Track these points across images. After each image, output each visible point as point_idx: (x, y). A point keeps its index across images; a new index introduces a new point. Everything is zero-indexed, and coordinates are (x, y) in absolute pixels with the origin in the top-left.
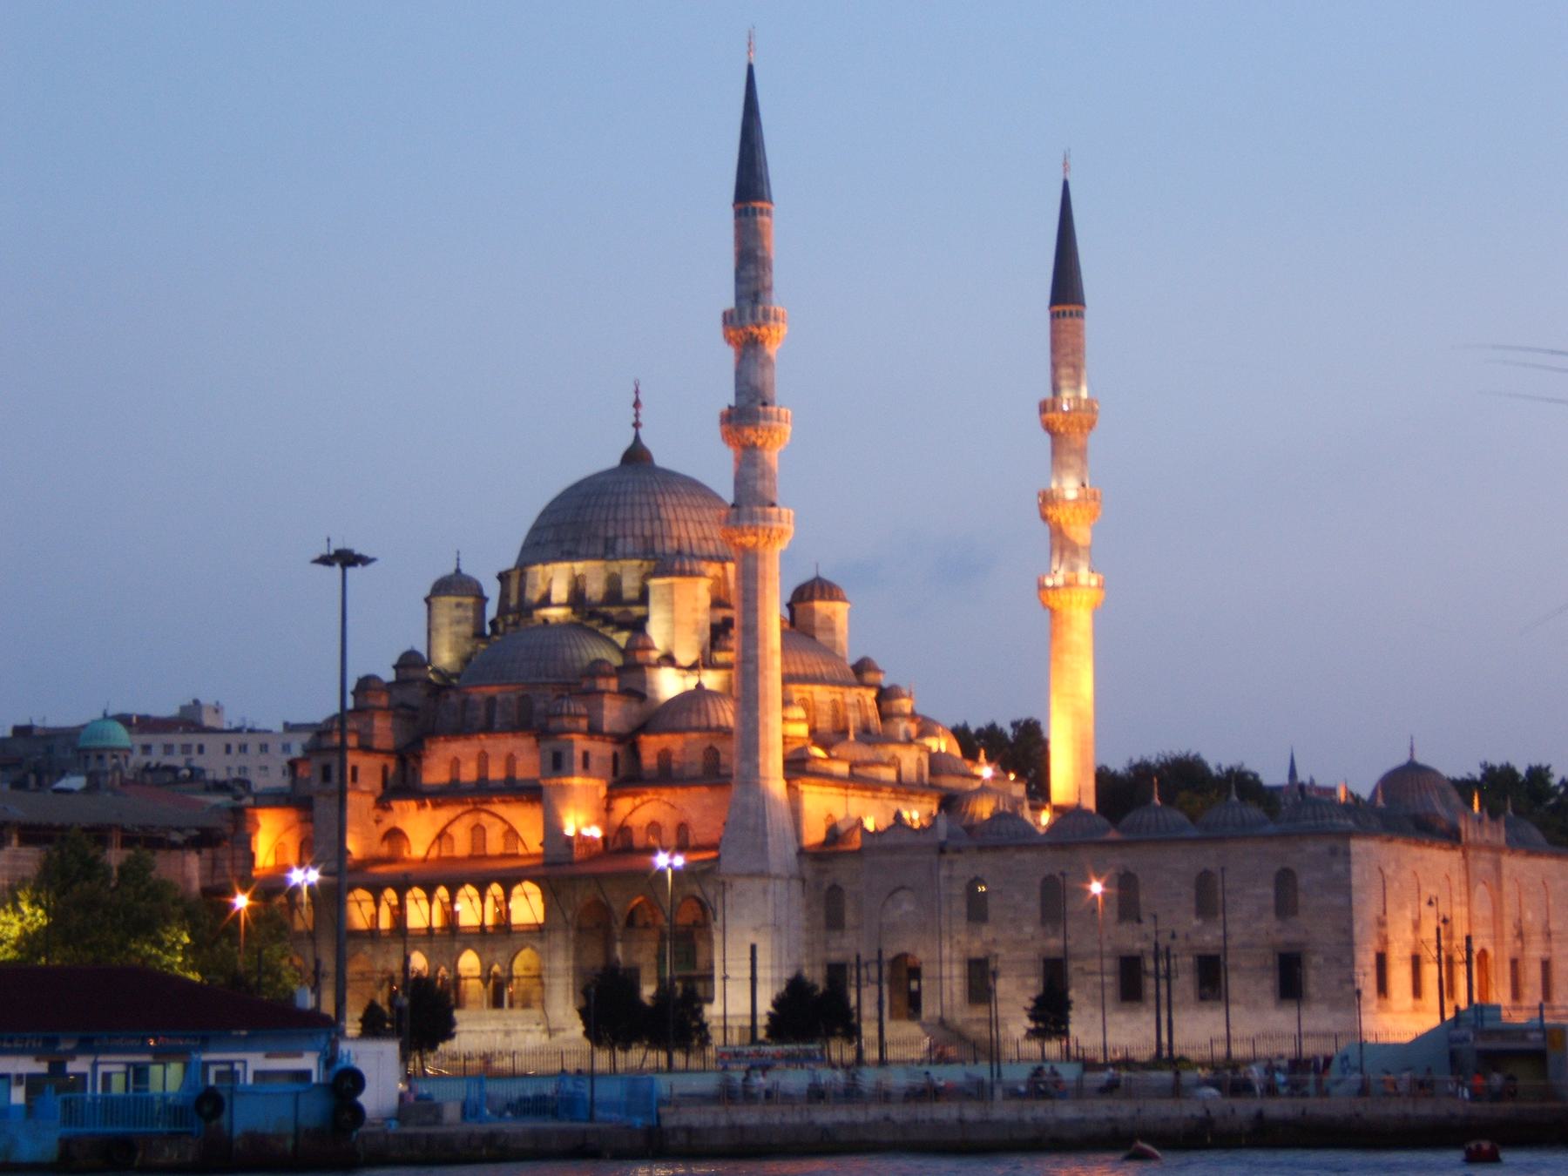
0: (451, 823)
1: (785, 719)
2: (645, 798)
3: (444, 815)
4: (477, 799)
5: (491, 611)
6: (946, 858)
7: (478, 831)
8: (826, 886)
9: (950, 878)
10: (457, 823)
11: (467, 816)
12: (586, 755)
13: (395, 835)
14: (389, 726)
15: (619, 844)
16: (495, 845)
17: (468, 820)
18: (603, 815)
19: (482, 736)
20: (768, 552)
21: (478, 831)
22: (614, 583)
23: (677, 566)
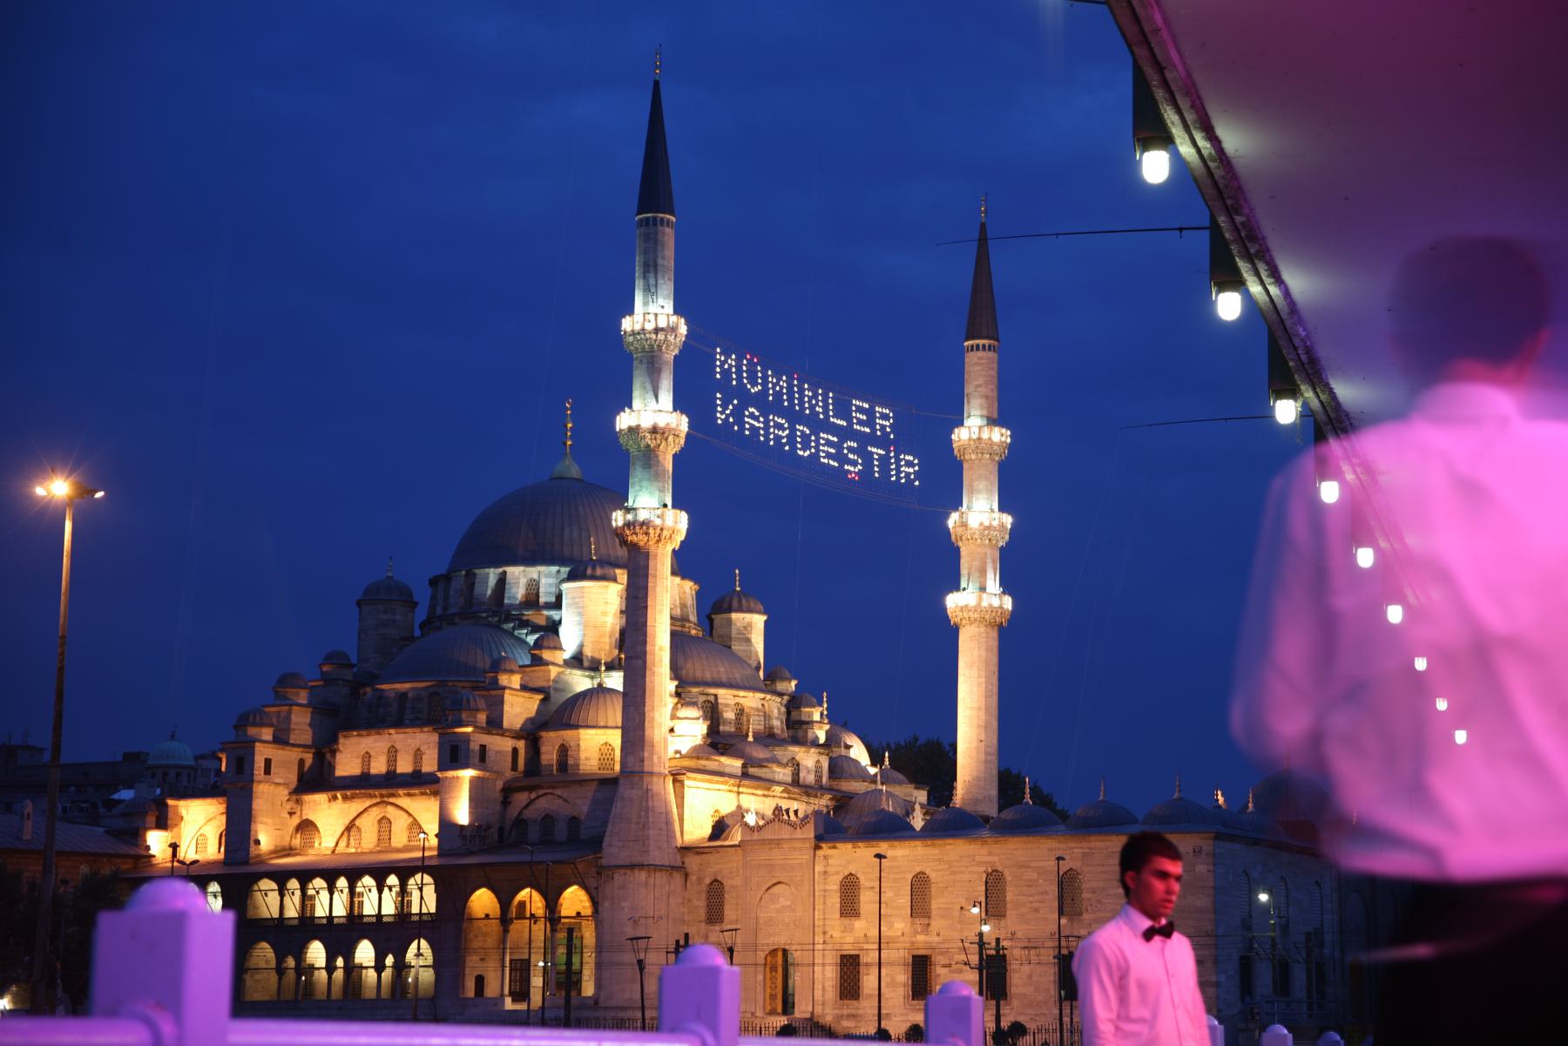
1: (673, 717)
2: (541, 792)
3: (356, 806)
4: (384, 792)
5: (421, 614)
6: (820, 853)
7: (385, 822)
8: (708, 880)
9: (825, 872)
10: (365, 815)
11: (375, 809)
13: (307, 827)
14: (308, 721)
16: (399, 837)
17: (376, 813)
19: (392, 731)
20: (660, 551)
21: (385, 822)
22: (533, 587)
23: (589, 572)
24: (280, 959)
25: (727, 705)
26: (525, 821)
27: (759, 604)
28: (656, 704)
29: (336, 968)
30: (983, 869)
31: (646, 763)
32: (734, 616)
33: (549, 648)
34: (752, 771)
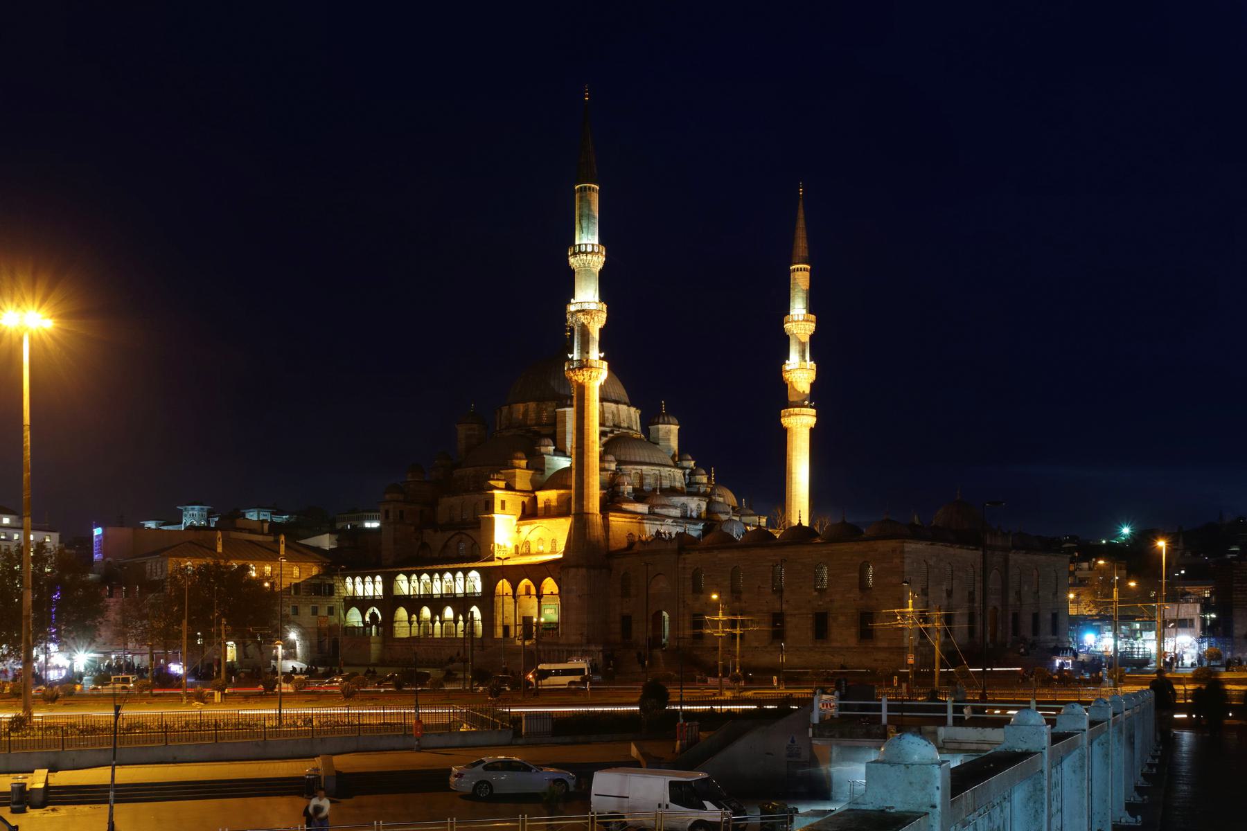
0: (449, 539)
2: (536, 525)
8: (622, 573)
9: (684, 568)
12: (503, 503)
15: (524, 550)
18: (516, 535)
24: (410, 616)
25: (648, 475)
26: (528, 541)
27: (675, 419)
28: (590, 474)
29: (435, 621)
30: (771, 564)
31: (585, 508)
32: (660, 426)
33: (544, 446)
34: (657, 510)
